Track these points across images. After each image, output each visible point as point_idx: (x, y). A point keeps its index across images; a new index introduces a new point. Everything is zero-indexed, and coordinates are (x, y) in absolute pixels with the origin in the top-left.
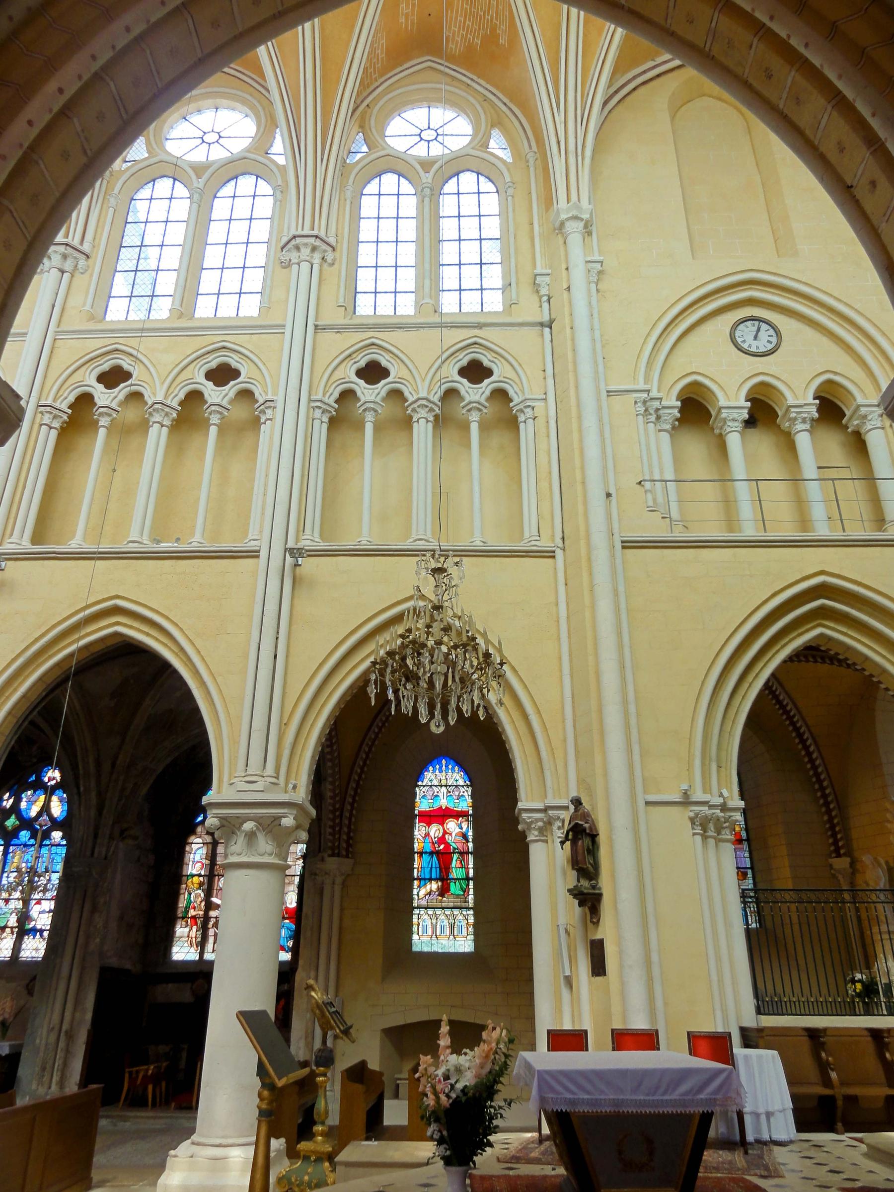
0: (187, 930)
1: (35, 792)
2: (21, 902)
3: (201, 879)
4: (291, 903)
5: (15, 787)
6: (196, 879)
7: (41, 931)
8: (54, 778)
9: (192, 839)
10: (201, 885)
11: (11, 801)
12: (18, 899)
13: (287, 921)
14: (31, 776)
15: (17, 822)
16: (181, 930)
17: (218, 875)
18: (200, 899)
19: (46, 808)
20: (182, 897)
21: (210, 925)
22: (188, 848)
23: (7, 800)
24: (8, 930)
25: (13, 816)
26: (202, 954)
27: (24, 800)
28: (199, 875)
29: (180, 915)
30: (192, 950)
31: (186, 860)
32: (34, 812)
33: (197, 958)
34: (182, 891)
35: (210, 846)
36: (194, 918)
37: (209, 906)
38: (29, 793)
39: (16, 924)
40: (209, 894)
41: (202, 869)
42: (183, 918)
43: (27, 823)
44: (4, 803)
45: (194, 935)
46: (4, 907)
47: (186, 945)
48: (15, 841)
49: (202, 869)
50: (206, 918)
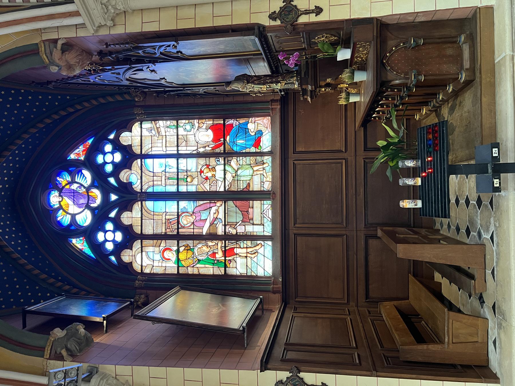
0: (238, 260)
3: (181, 249)
4: (208, 136)
6: (182, 256)
9: (137, 267)
10: (188, 249)
13: (228, 138)
16: (239, 267)
17: (178, 228)
18: (205, 248)
20: (203, 271)
21: (234, 232)
22: (147, 271)
26: (264, 238)
28: (178, 251)
29: (223, 270)
30: (261, 251)
31: (160, 271)
33: (270, 243)
34: (196, 272)
35: (145, 242)
36: (225, 253)
37: (212, 236)
40: (199, 237)
41: (171, 250)
42: (225, 267)
45: (244, 250)
47: (255, 259)
49: (171, 250)
50: (226, 237)
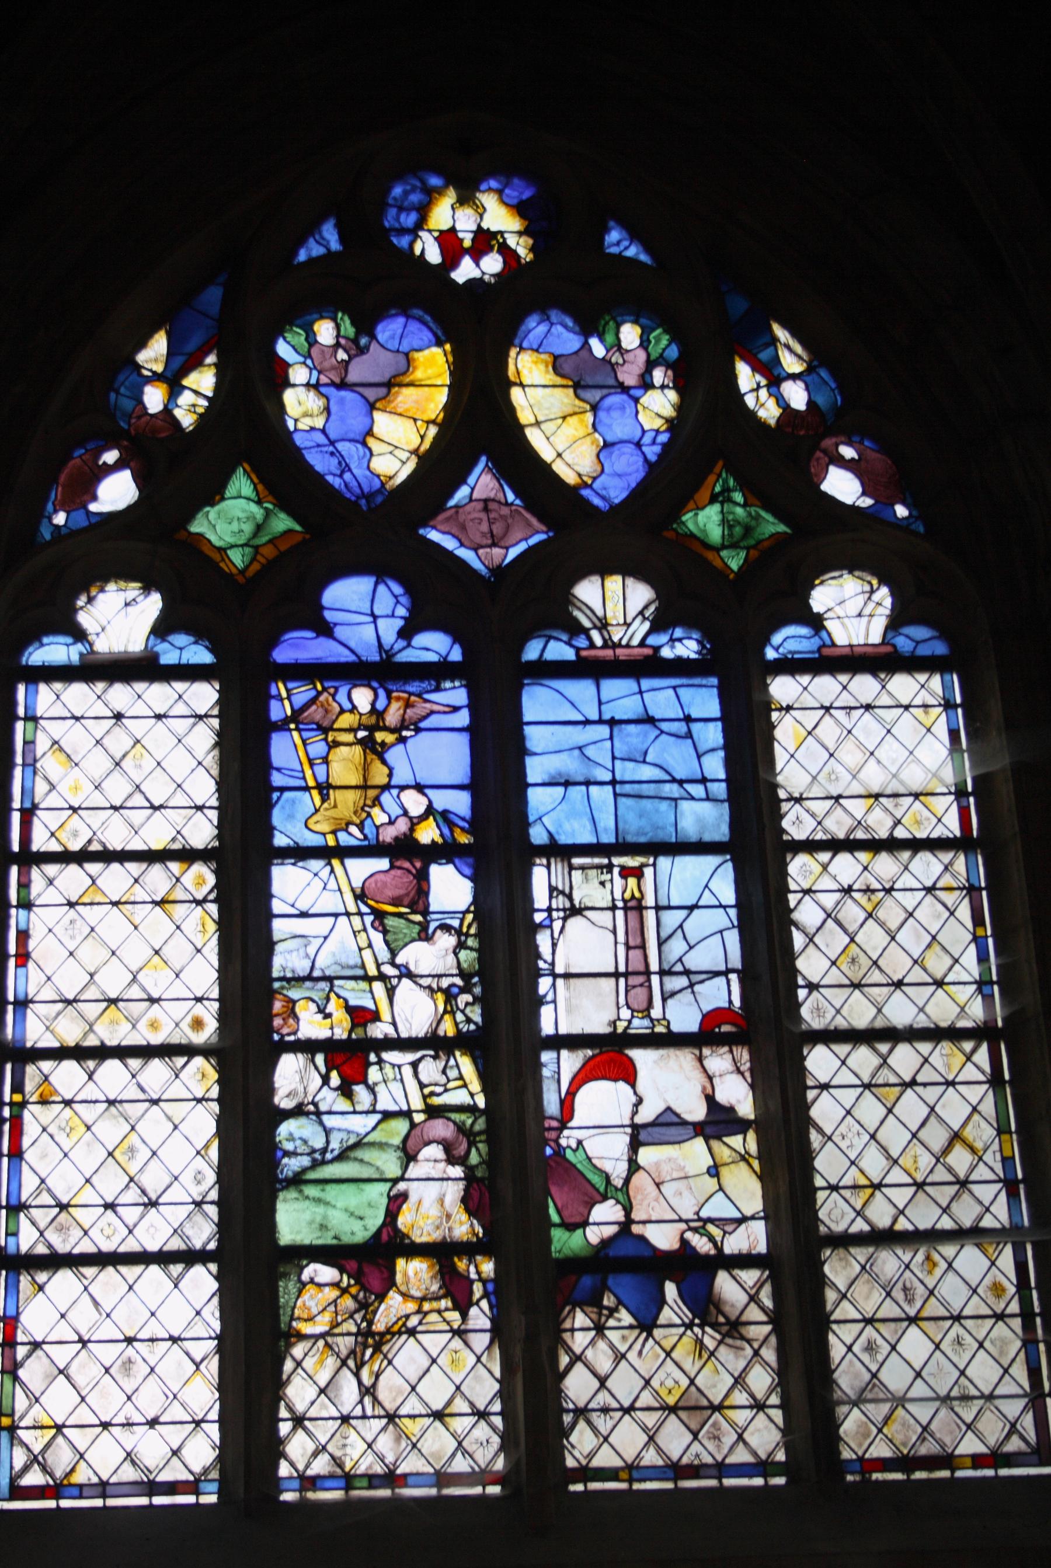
1: (366, 326)
2: (466, 1064)
5: (213, 296)
7: (693, 1269)
8: (485, 241)
11: (203, 381)
12: (434, 1043)
14: (311, 229)
15: (283, 523)
19: (480, 424)
23: (173, 381)
24: (415, 1272)
25: (241, 484)
27: (299, 374)
32: (395, 445)
38: (325, 332)
39: (463, 1227)
43: (346, 527)
44: (154, 398)
46: (329, 1099)
48: (298, 647)
